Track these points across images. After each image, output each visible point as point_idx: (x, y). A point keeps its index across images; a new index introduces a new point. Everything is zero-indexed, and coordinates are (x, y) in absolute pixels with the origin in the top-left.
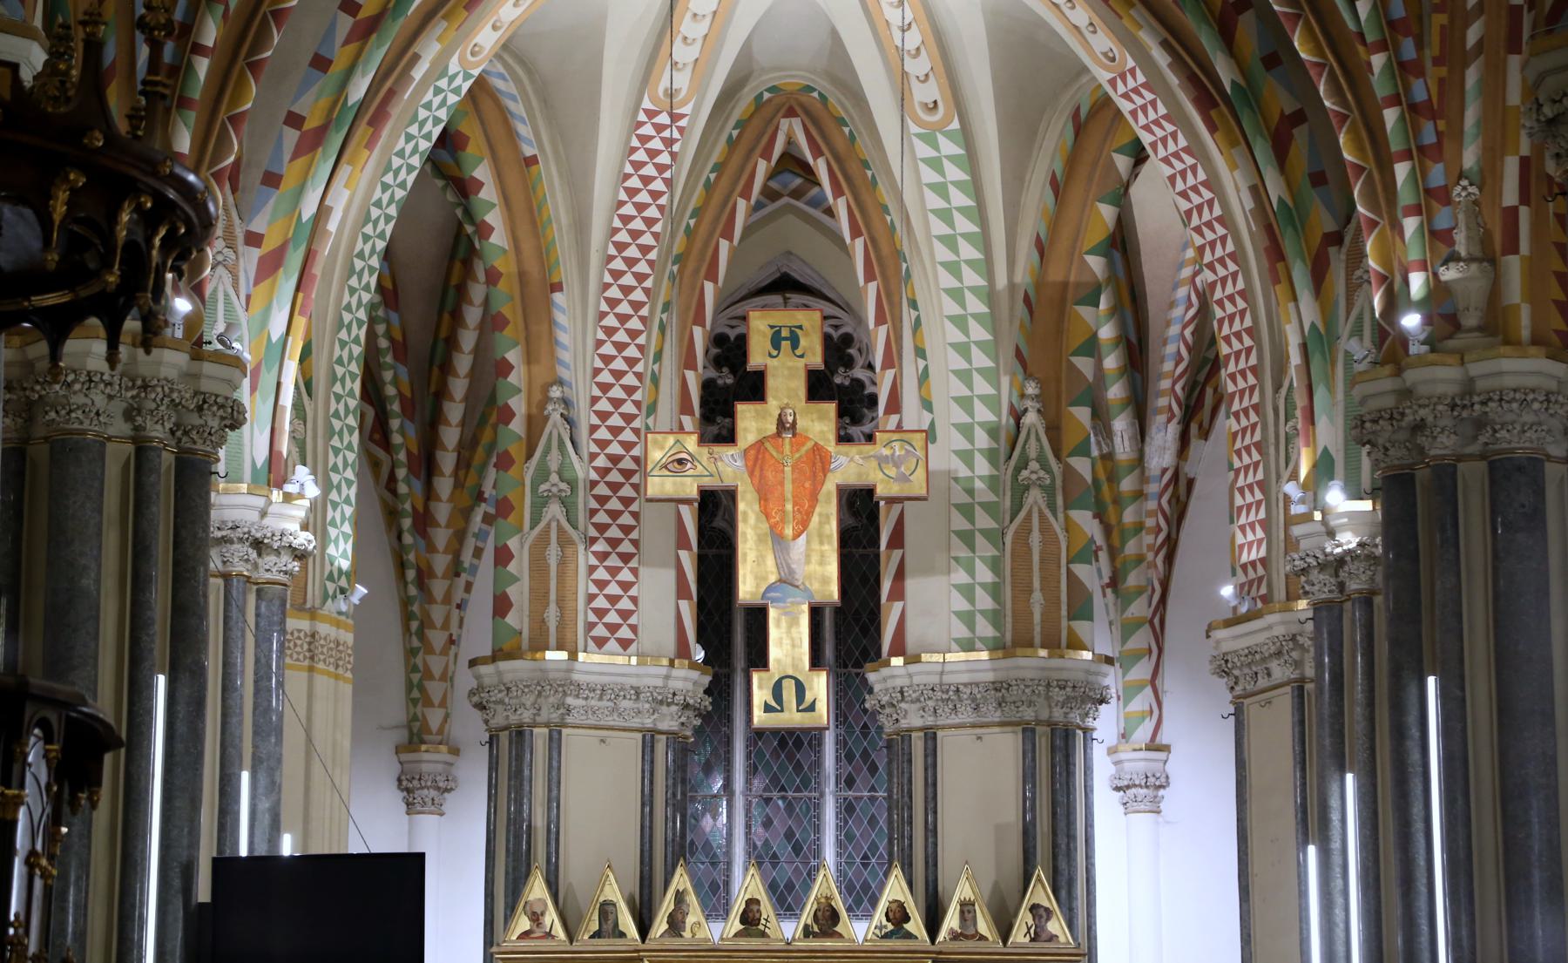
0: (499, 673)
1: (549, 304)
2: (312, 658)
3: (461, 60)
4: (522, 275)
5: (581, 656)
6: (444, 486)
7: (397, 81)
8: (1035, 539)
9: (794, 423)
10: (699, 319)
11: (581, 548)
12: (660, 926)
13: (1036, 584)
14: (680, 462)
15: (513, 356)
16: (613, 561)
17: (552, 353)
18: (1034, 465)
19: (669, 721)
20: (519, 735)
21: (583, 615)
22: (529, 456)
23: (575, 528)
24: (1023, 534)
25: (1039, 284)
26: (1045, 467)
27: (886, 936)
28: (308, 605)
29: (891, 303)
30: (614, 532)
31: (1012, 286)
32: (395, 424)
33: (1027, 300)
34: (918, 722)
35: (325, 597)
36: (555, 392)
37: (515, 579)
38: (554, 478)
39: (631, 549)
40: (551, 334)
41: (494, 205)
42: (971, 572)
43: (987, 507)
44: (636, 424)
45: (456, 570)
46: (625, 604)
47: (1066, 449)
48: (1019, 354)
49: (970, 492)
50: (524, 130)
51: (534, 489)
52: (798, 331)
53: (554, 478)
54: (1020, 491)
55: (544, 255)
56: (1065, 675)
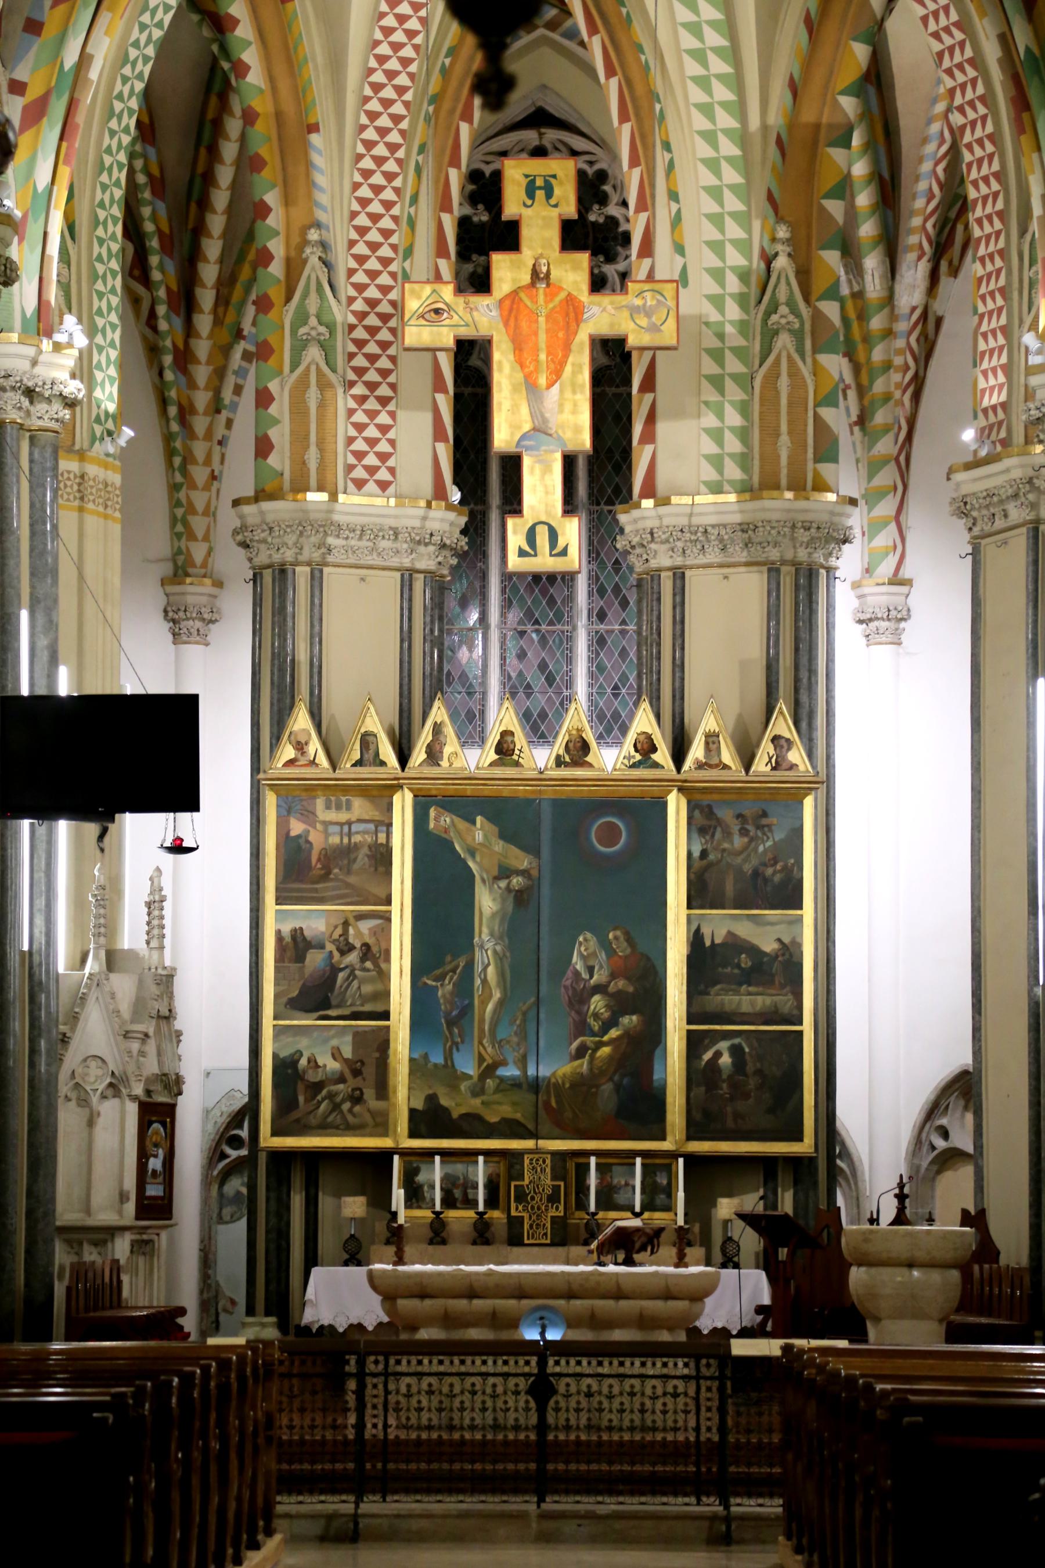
0: (262, 513)
1: (306, 146)
2: (82, 499)
4: (279, 116)
5: (342, 498)
6: (204, 322)
8: (784, 383)
10: (455, 162)
11: (340, 391)
12: (419, 755)
13: (784, 427)
14: (437, 311)
15: (271, 198)
16: (372, 404)
17: (309, 195)
18: (783, 309)
19: (427, 560)
20: (282, 573)
21: (343, 457)
22: (288, 299)
23: (334, 370)
24: (773, 377)
25: (792, 125)
26: (795, 311)
27: (634, 766)
28: (77, 447)
30: (372, 376)
31: (765, 127)
32: (154, 260)
33: (779, 142)
34: (667, 562)
35: (93, 439)
36: (313, 235)
37: (276, 422)
38: (313, 321)
39: (389, 393)
40: (308, 175)
41: (250, 43)
42: (720, 415)
43: (737, 351)
44: (393, 267)
45: (216, 407)
46: (383, 447)
47: (815, 293)
48: (770, 197)
49: (721, 336)
51: (294, 332)
52: (553, 181)
53: (313, 321)
54: (769, 335)
55: (301, 94)
56: (809, 517)
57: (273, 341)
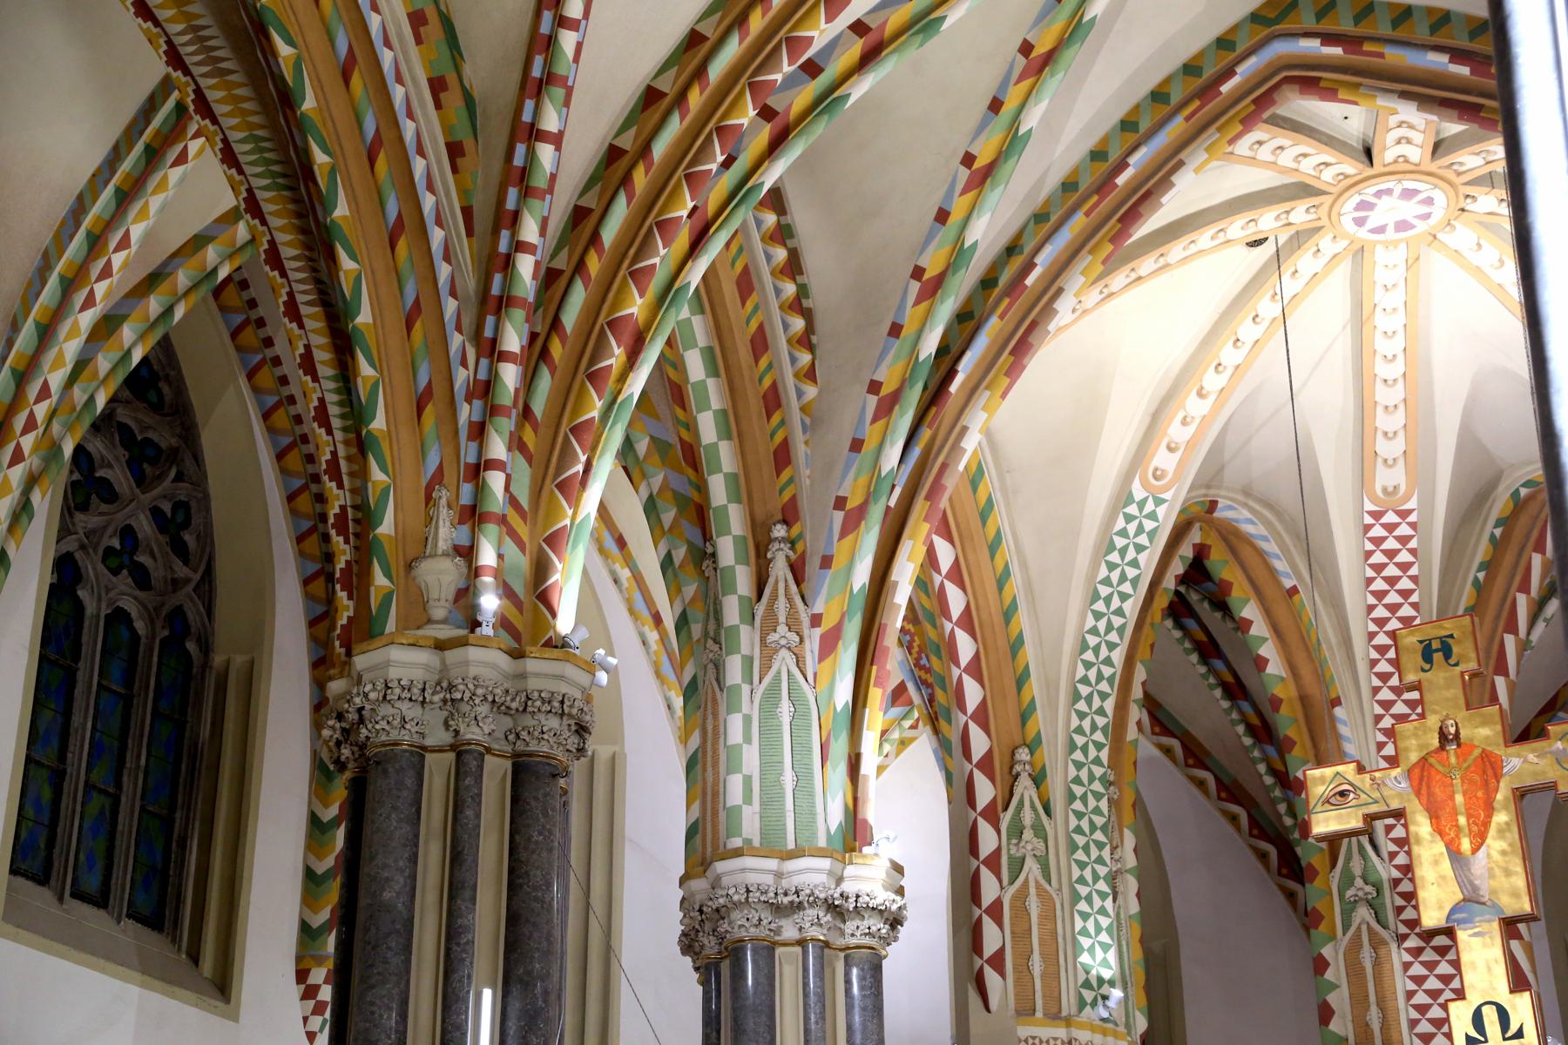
1: (1333, 719)
3: (1145, 485)
4: (1304, 699)
7: (948, 456)
11: (1394, 946)
14: (1343, 794)
16: (1429, 955)
22: (1333, 865)
23: (1385, 927)
28: (1064, 1013)
35: (1082, 1004)
37: (1334, 987)
38: (1359, 882)
41: (1265, 640)
50: (1280, 565)
51: (1341, 896)
52: (1450, 641)
53: (1359, 882)
57: (1321, 907)
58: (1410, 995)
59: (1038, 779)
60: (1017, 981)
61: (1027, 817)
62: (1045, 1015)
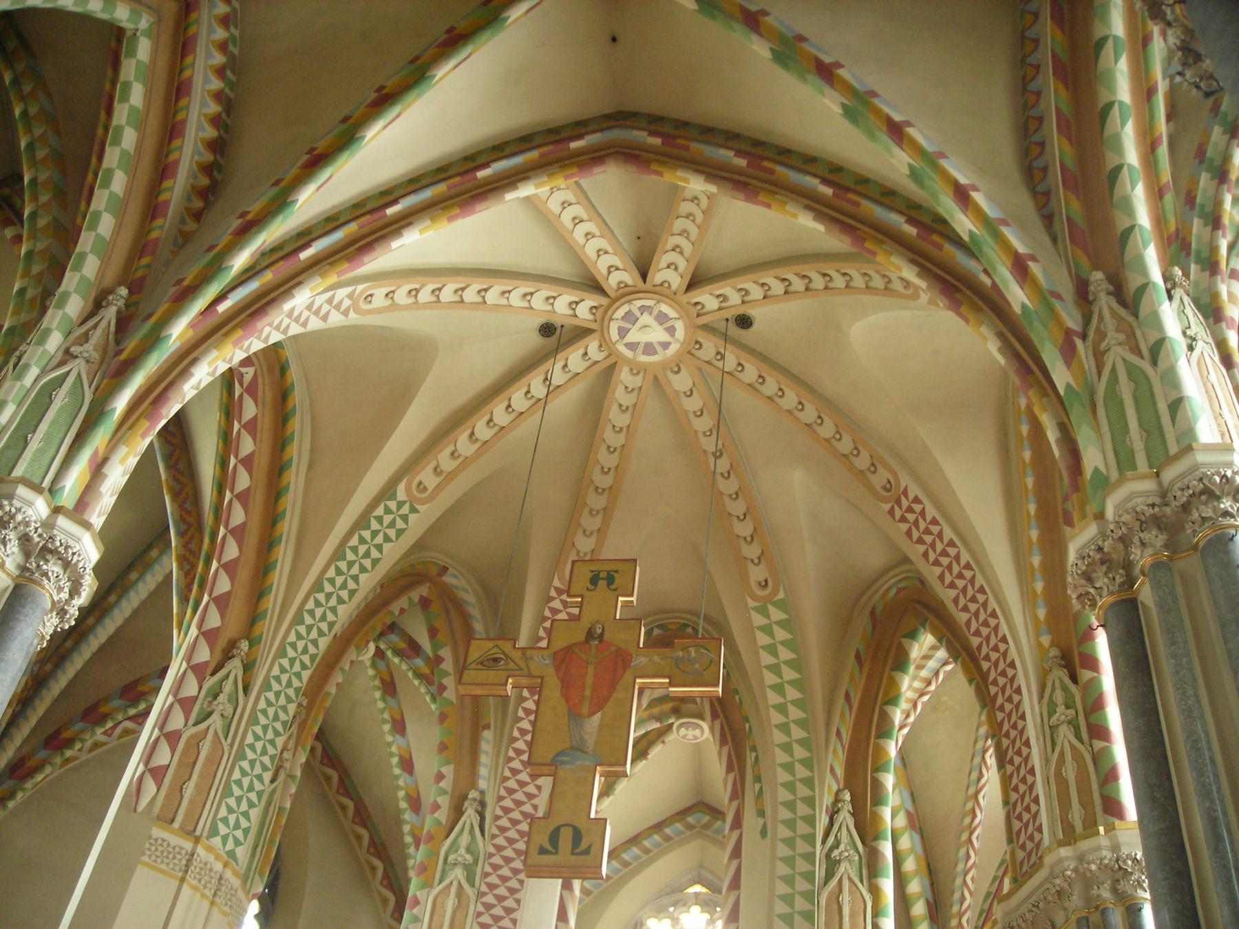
2: (186, 872)
3: (408, 489)
9: (602, 635)
14: (496, 660)
23: (473, 885)
28: (198, 833)
29: (738, 757)
36: (473, 794)
41: (450, 674)
52: (615, 575)
53: (462, 851)
58: (479, 914)
59: (248, 667)
60: (167, 796)
61: (228, 687)
62: (181, 828)
